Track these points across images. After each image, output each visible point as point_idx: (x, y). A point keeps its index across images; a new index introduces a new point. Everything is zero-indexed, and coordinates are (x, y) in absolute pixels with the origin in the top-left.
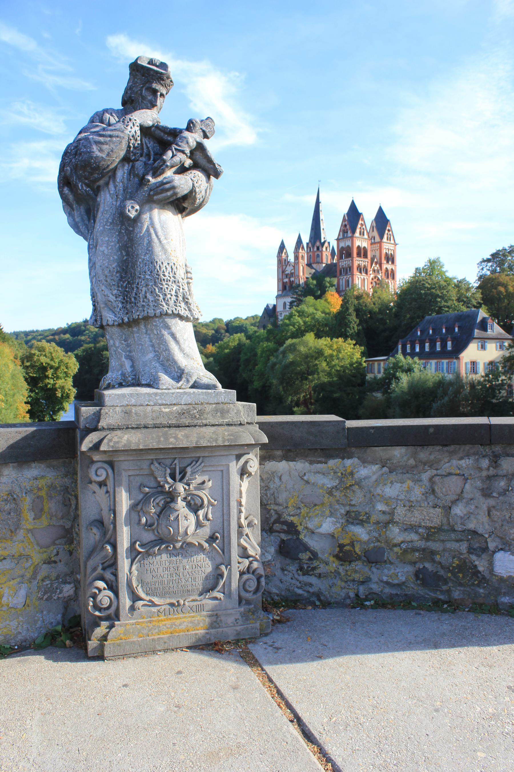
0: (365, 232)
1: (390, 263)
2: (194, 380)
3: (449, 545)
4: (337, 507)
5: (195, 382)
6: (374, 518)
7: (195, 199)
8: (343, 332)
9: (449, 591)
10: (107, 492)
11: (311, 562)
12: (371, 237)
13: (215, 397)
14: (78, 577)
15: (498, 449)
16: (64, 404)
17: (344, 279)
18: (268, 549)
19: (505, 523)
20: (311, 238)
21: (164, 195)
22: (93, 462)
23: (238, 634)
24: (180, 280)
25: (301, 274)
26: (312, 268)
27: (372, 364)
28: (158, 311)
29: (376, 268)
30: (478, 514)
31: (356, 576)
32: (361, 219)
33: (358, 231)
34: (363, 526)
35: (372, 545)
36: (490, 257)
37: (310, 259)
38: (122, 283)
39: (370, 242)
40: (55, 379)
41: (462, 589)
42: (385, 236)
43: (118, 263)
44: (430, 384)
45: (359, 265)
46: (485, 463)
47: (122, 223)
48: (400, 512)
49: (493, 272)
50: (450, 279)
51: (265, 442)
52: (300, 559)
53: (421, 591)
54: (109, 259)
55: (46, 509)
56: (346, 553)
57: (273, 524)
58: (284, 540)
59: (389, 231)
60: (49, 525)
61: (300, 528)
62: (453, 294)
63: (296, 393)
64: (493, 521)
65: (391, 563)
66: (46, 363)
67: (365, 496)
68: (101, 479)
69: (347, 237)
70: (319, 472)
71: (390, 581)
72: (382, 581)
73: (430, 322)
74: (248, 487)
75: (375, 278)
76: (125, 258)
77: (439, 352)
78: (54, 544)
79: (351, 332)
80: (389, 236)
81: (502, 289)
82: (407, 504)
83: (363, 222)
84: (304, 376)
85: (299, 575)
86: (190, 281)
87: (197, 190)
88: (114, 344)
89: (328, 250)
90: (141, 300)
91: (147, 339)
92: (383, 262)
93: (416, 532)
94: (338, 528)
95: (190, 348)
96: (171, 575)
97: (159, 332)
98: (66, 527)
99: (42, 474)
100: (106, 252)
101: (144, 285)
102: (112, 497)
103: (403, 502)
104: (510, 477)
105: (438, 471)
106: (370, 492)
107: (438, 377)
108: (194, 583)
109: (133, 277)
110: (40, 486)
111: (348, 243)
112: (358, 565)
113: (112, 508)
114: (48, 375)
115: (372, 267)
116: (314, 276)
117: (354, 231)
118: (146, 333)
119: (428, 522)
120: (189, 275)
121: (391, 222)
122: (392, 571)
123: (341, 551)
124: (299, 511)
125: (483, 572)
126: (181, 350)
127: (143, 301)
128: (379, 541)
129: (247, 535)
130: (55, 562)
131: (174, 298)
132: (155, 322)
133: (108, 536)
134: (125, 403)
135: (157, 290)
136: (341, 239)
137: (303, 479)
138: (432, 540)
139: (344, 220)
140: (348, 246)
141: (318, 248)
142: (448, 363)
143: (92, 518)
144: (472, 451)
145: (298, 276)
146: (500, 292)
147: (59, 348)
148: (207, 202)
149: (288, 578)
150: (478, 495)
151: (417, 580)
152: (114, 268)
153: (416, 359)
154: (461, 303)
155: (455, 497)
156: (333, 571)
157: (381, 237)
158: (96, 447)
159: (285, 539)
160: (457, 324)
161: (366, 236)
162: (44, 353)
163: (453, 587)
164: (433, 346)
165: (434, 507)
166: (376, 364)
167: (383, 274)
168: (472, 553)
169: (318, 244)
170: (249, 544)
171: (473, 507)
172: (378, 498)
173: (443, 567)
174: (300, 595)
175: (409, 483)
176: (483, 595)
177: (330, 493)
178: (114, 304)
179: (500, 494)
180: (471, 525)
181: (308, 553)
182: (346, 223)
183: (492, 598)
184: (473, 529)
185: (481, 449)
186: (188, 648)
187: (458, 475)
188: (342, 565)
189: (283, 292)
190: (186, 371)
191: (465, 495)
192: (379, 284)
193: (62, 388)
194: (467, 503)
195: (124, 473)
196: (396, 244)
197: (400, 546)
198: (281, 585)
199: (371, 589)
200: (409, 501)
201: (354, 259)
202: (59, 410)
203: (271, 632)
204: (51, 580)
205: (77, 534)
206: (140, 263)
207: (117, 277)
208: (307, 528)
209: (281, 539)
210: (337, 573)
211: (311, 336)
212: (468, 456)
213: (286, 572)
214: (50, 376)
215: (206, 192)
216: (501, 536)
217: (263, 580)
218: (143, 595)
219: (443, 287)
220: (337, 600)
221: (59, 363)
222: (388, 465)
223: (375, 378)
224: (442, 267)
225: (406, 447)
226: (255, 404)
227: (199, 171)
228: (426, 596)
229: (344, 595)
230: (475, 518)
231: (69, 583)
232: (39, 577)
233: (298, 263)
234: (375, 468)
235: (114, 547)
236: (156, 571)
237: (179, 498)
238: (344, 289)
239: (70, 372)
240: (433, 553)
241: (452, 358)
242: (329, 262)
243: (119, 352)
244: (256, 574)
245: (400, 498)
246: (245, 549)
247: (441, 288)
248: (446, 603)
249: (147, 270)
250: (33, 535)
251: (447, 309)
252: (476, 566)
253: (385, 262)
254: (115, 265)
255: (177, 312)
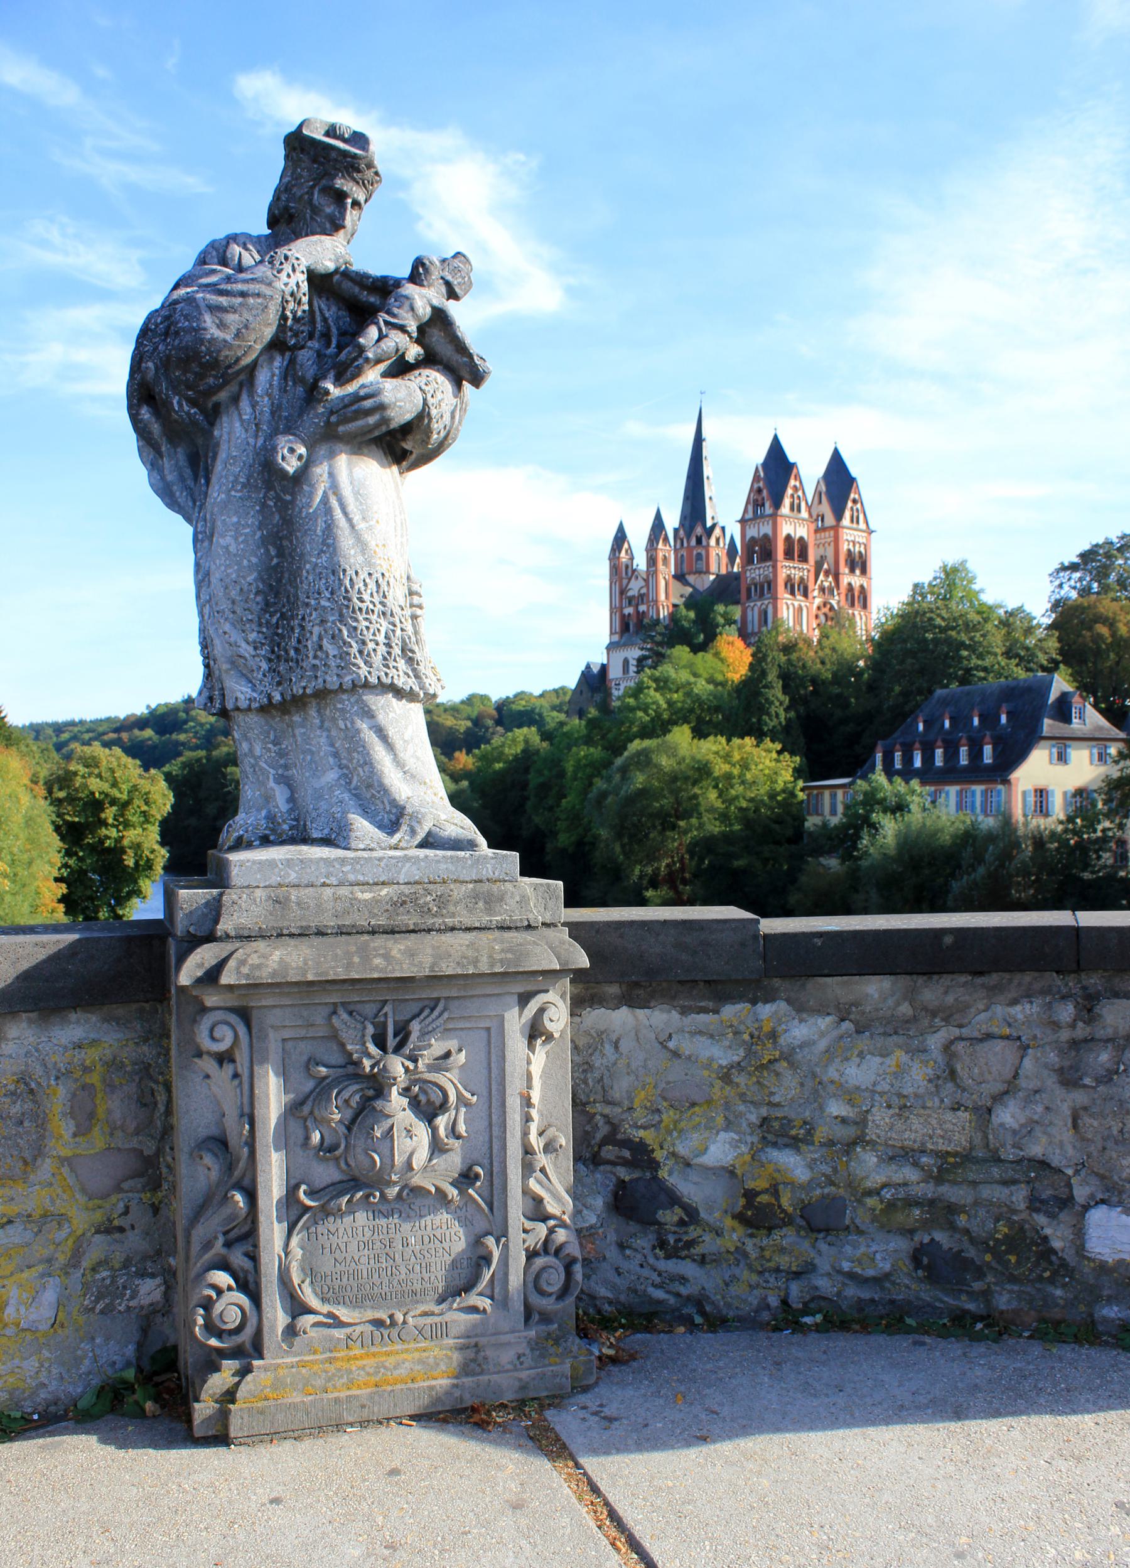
0: (803, 505)
1: (858, 572)
2: (426, 829)
3: (986, 1192)
4: (742, 1108)
5: (429, 834)
6: (822, 1133)
7: (428, 431)
8: (753, 724)
9: (986, 1294)
10: (236, 1075)
11: (684, 1229)
12: (815, 517)
13: (472, 866)
14: (172, 1261)
15: (1094, 981)
16: (141, 883)
17: (756, 609)
18: (590, 1201)
19: (1110, 1144)
20: (683, 518)
21: (360, 423)
22: (204, 1010)
23: (524, 1388)
24: (397, 610)
25: (662, 597)
26: (686, 583)
27: (817, 795)
28: (348, 679)
29: (826, 584)
30: (1051, 1123)
31: (784, 1261)
32: (793, 477)
33: (787, 501)
34: (798, 1150)
35: (818, 1192)
36: (1076, 560)
37: (682, 563)
38: (267, 616)
39: (813, 527)
40: (121, 828)
41: (1016, 1288)
42: (847, 514)
43: (259, 573)
44: (946, 839)
45: (789, 576)
46: (1066, 1012)
47: (269, 486)
48: (880, 1119)
50: (990, 608)
51: (584, 966)
52: (660, 1224)
53: (926, 1293)
54: (239, 564)
55: (101, 1112)
56: (762, 1209)
57: (600, 1146)
58: (623, 1181)
59: (855, 501)
60: (108, 1149)
61: (659, 1155)
62: (997, 641)
63: (652, 856)
64: (1083, 1139)
65: (860, 1232)
66: (100, 793)
67: (802, 1085)
68: (222, 1047)
69: (763, 516)
70: (701, 1033)
71: (859, 1270)
72: (840, 1272)
73: (945, 702)
74: (545, 1065)
75: (825, 604)
76: (275, 561)
77: (965, 769)
78: (118, 1189)
79: (772, 724)
80: (855, 514)
81: (1104, 630)
82: (895, 1101)
83: (798, 484)
84: (668, 821)
85: (657, 1258)
86: (419, 612)
87: (434, 412)
88: (251, 750)
89: (721, 545)
90: (311, 655)
91: (323, 740)
92: (841, 571)
93: (916, 1164)
94: (742, 1154)
95: (418, 758)
96: (377, 1258)
97: (349, 725)
98: (145, 1153)
99: (92, 1036)
100: (232, 549)
101: (317, 621)
102: (246, 1087)
103: (885, 1097)
104: (1121, 1042)
105: (963, 1030)
106: (814, 1075)
107: (964, 822)
108: (426, 1276)
109: (293, 603)
110: (88, 1062)
111: (766, 529)
112: (786, 1237)
113: (246, 1110)
114: (106, 819)
115: (819, 582)
116: (691, 602)
117: (777, 504)
118: (321, 727)
119: (941, 1141)
120: (416, 600)
121: (861, 482)
122: (863, 1249)
123: (749, 1204)
124: (657, 1118)
125: (1063, 1250)
126: (399, 763)
127: (315, 657)
128: (832, 1183)
129: (543, 1170)
130: (121, 1230)
131: (382, 649)
132: (342, 702)
133: (237, 1173)
134: (275, 880)
135: (345, 633)
136: (750, 520)
137: (666, 1047)
138: (948, 1181)
139: (756, 478)
140: (766, 536)
141: (699, 541)
142: (985, 793)
143: (203, 1132)
144: (1037, 986)
145: (656, 601)
146: (1100, 636)
147: (130, 760)
148: (454, 440)
149: (633, 1266)
150: (1051, 1081)
151: (916, 1269)
152: (250, 584)
153: (915, 783)
154: (1014, 661)
155: (1000, 1087)
156: (732, 1249)
157: (839, 515)
158: (212, 976)
159: (627, 1179)
160: (1004, 708)
161: (804, 514)
162: (96, 771)
163: (995, 1284)
164: (951, 754)
165: (954, 1109)
166: (827, 794)
167: (843, 597)
168: (1037, 1210)
169: (699, 530)
170: (548, 1190)
171: (1040, 1109)
172: (831, 1088)
173: (972, 1240)
174: (660, 1302)
175: (900, 1056)
176: (1061, 1302)
177: (726, 1077)
178: (251, 663)
179: (1099, 1081)
180: (1036, 1150)
181: (677, 1210)
182: (761, 484)
183: (1082, 1308)
184: (1040, 1156)
185: (1057, 980)
186: (412, 1417)
187: (1007, 1038)
188: (751, 1236)
189: (621, 637)
190: (409, 810)
191: (1023, 1083)
192: (832, 618)
193: (137, 847)
194: (1028, 1101)
195: (272, 1035)
196: (870, 532)
197: (878, 1194)
198: (617, 1280)
199: (816, 1288)
200: (900, 1096)
201: (779, 565)
202: (130, 895)
203: (596, 1383)
204: (112, 1269)
205: (169, 1167)
206: (308, 572)
207: (258, 603)
208: (674, 1154)
209: (618, 1178)
210: (741, 1253)
211: (683, 734)
212: (1029, 996)
213: (628, 1252)
214: (110, 821)
215: (453, 417)
216: (1101, 1172)
217: (578, 1269)
218: (313, 1302)
219: (974, 626)
220: (740, 1313)
221: (129, 792)
222: (852, 1017)
223: (825, 825)
224: (971, 581)
225: (893, 977)
226: (561, 883)
227: (438, 371)
228: (937, 1304)
229: (755, 1302)
230: (1045, 1133)
231: (153, 1276)
232: (86, 1263)
233: (656, 572)
234: (824, 1022)
235: (251, 1196)
236: (343, 1249)
237: (394, 1090)
238: (756, 630)
239: (154, 811)
240: (952, 1209)
241: (994, 782)
242: (723, 571)
243: (261, 769)
244: (562, 1255)
245: (879, 1088)
246: (538, 1201)
247: (969, 627)
248: (981, 1318)
249: (323, 588)
250: (72, 1170)
251: (982, 674)
252: (1046, 1239)
253: (847, 571)
254: (252, 577)
255: (389, 681)
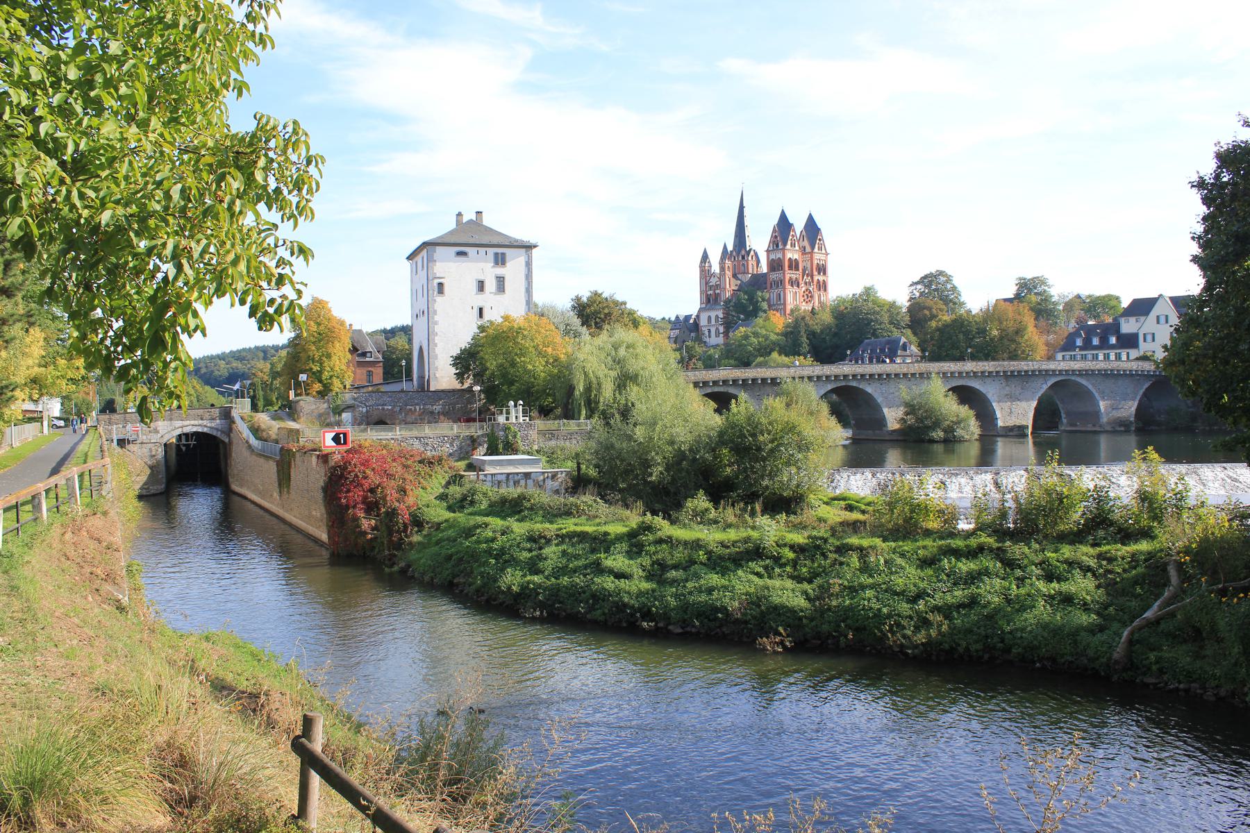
20: (735, 246)
26: (737, 279)
33: (789, 242)
49: (922, 294)
62: (886, 319)
73: (868, 344)
81: (927, 312)
111: (780, 255)
117: (785, 244)
139: (774, 231)
141: (743, 257)
157: (813, 248)
161: (797, 248)
169: (743, 252)
247: (875, 313)
